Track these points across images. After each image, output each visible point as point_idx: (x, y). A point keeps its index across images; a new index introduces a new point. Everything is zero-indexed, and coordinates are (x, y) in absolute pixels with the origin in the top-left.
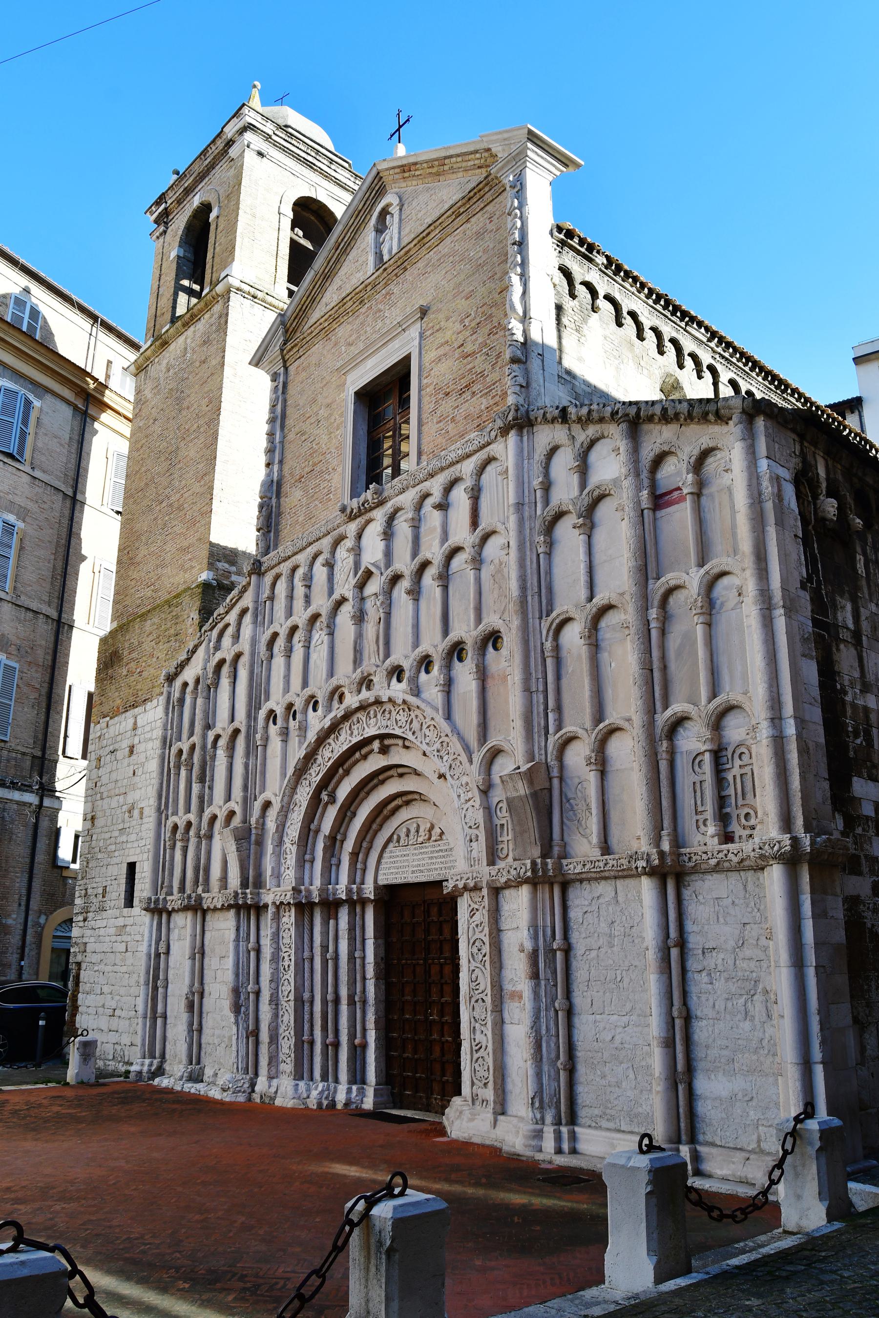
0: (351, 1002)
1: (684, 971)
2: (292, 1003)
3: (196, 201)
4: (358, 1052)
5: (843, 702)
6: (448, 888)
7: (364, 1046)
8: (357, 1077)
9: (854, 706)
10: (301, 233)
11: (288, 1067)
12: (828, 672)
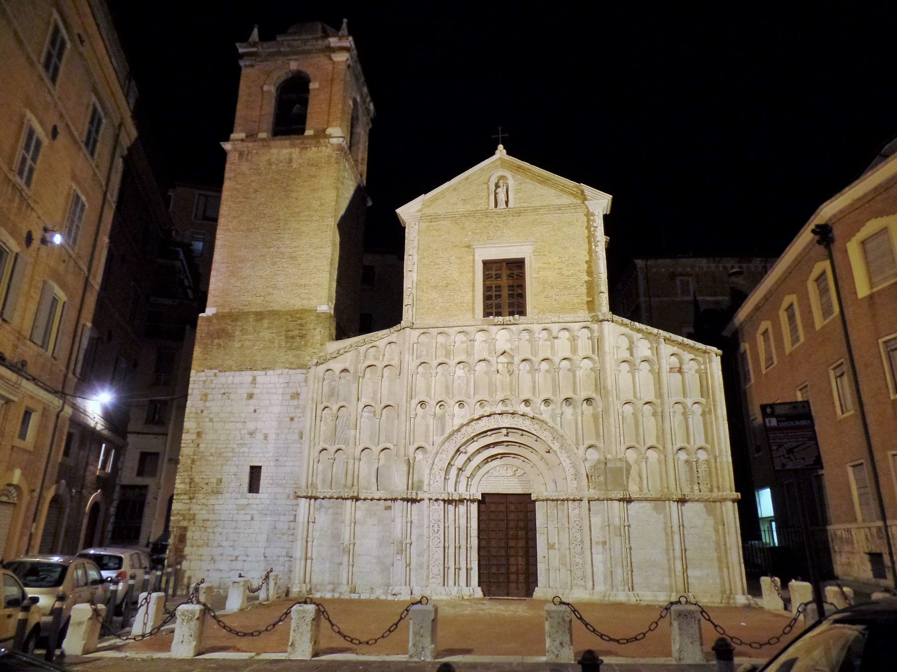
3: (294, 66)
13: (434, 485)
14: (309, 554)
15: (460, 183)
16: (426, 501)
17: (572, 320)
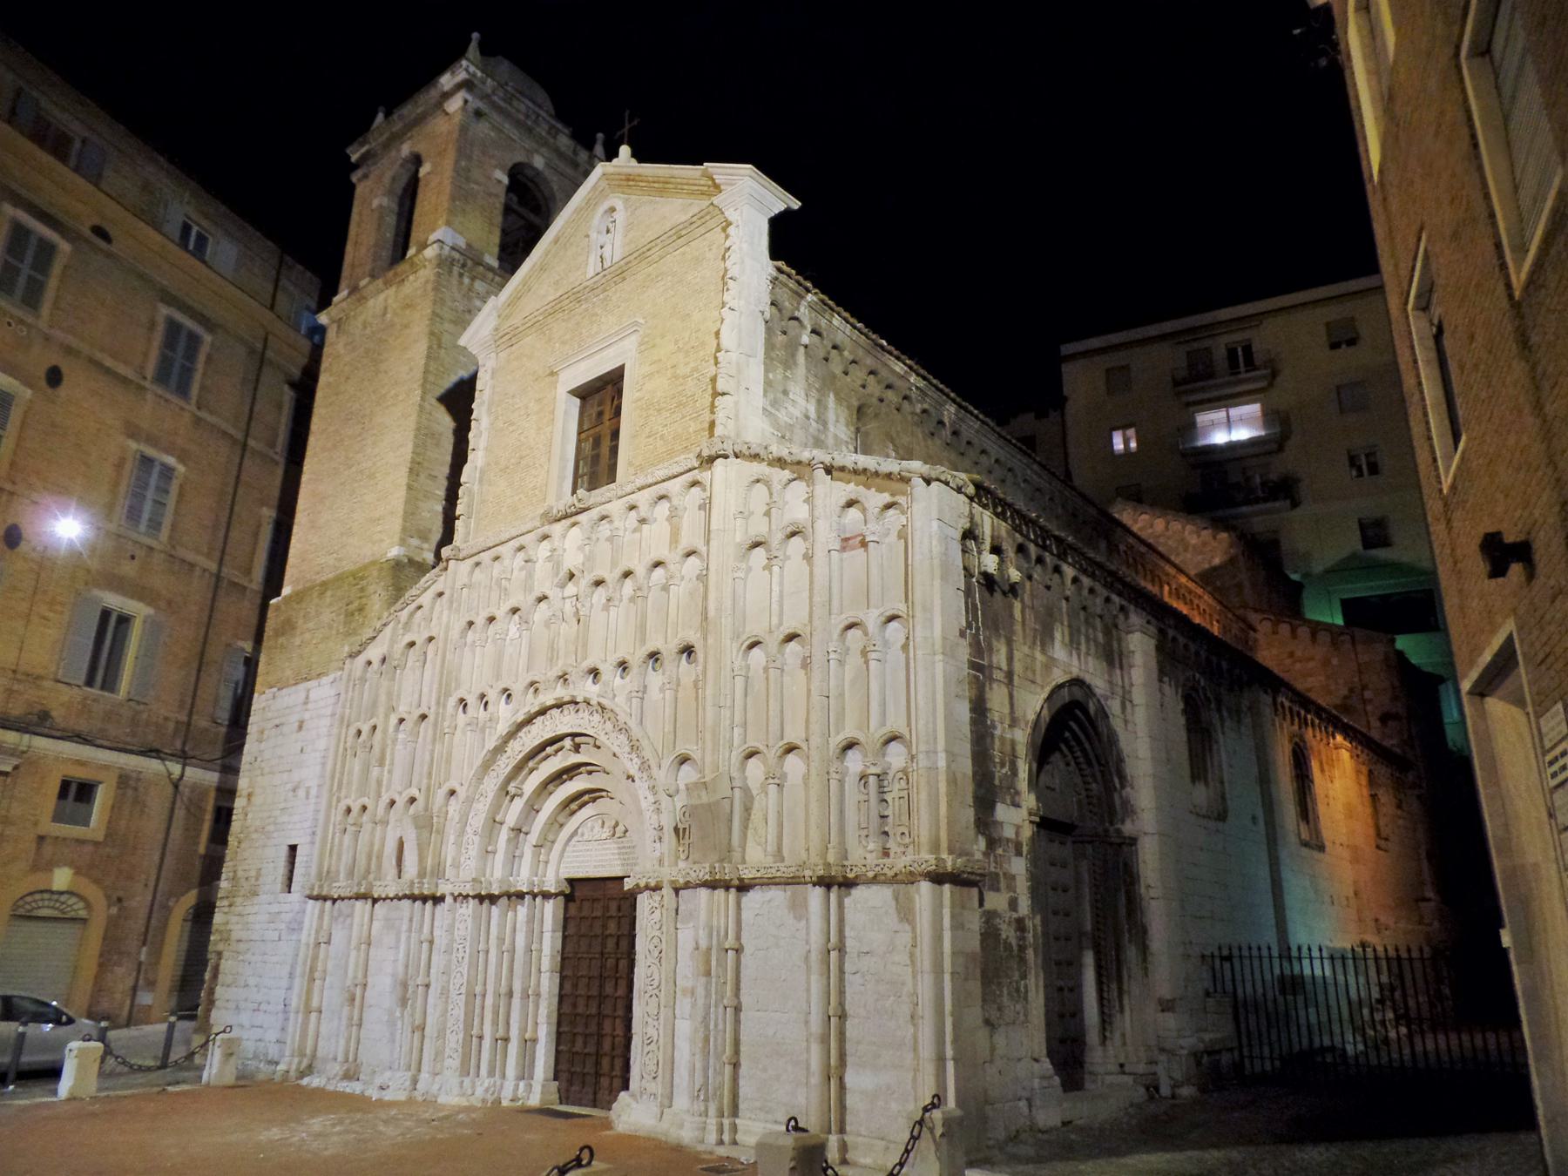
0: (525, 996)
1: (841, 971)
2: (463, 997)
3: (406, 149)
4: (528, 1044)
5: (992, 736)
6: (628, 885)
7: (535, 1041)
8: (525, 1073)
9: (1002, 739)
10: (515, 199)
11: (453, 1063)
12: (979, 708)
13: (463, 866)
14: (315, 1003)
15: (547, 253)
16: (449, 899)
17: (669, 473)
